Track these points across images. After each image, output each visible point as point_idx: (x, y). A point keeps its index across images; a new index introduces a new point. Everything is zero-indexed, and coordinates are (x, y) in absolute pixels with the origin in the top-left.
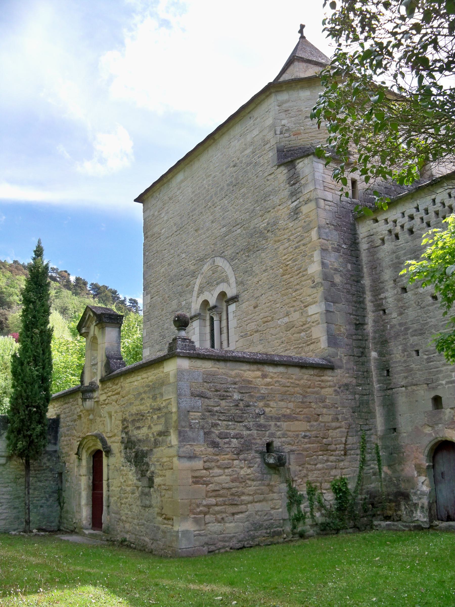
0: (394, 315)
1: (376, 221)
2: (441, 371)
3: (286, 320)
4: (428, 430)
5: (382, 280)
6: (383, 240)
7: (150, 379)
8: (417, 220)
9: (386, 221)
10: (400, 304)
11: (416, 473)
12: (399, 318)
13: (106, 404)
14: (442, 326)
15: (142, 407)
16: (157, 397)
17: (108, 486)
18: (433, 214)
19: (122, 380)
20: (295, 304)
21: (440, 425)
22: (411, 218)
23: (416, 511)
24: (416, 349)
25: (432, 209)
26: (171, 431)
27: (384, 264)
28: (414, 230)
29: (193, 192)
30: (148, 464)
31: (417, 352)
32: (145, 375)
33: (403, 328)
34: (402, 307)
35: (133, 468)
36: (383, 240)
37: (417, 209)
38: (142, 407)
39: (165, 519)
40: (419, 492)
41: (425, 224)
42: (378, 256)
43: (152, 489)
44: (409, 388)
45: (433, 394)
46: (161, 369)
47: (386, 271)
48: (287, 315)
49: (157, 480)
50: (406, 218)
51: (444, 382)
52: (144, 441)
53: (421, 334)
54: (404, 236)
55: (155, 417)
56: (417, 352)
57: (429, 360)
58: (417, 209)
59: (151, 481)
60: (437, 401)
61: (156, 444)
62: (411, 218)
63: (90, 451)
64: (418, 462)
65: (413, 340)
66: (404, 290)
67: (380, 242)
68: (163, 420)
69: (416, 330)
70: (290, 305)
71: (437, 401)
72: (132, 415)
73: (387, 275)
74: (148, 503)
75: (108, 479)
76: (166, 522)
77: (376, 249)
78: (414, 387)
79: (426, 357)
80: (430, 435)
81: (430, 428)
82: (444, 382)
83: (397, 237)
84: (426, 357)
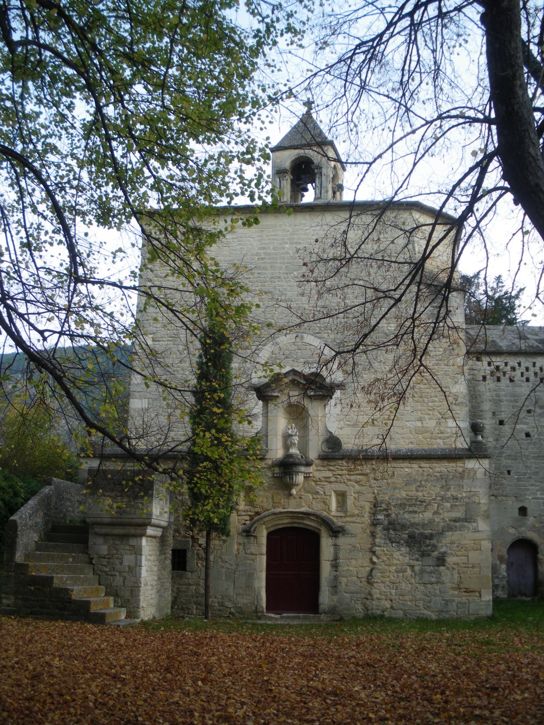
0: (491, 439)
1: (478, 359)
2: (528, 489)
3: (419, 424)
4: (512, 531)
5: (481, 409)
6: (484, 378)
7: (437, 469)
8: (518, 373)
9: (489, 364)
10: (497, 432)
11: (498, 562)
12: (495, 442)
13: (330, 482)
14: (533, 457)
15: (420, 494)
16: (450, 488)
17: (335, 566)
18: (533, 374)
19: (374, 463)
20: (431, 412)
21: (523, 528)
22: (513, 369)
23: (497, 590)
24: (509, 469)
25: (532, 369)
26: (479, 519)
27: (485, 397)
28: (515, 379)
29: (264, 248)
30: (435, 547)
31: (509, 472)
32: (423, 465)
33: (497, 451)
34: (498, 435)
35: (404, 549)
36: (484, 378)
37: (519, 364)
38: (420, 494)
39: (466, 592)
40: (500, 576)
41: (524, 379)
42: (479, 388)
43: (442, 568)
44: (499, 498)
45: (520, 505)
46: (460, 464)
47: (486, 403)
48: (420, 420)
49: (450, 560)
50: (509, 368)
51: (530, 498)
52: (424, 525)
53: (514, 459)
54: (505, 381)
55: (448, 505)
56: (509, 472)
57: (519, 480)
58: (519, 364)
59: (441, 561)
60: (523, 511)
61: (450, 528)
62: (513, 369)
63: (272, 529)
64: (501, 553)
65: (504, 462)
66: (501, 423)
67: (481, 378)
68: (464, 508)
69: (509, 456)
70: (424, 412)
71: (523, 511)
72: (398, 499)
73: (487, 406)
74: (433, 580)
75: (336, 558)
76: (466, 594)
77: (477, 382)
78: (504, 498)
79: (516, 477)
80: (514, 534)
81: (514, 530)
82: (530, 498)
83: (499, 380)
84: (516, 477)
